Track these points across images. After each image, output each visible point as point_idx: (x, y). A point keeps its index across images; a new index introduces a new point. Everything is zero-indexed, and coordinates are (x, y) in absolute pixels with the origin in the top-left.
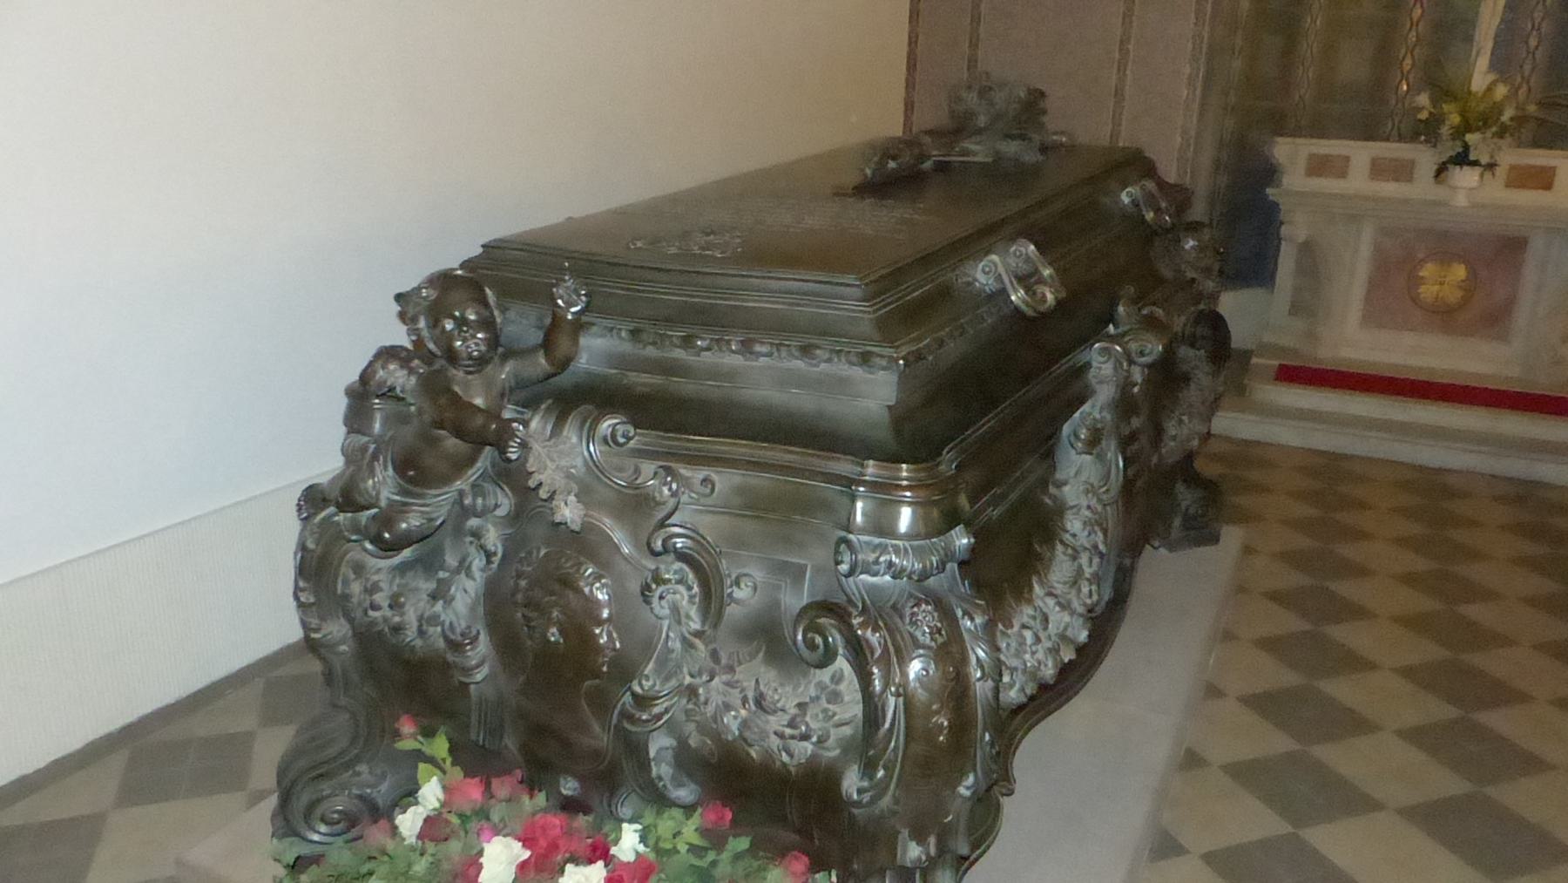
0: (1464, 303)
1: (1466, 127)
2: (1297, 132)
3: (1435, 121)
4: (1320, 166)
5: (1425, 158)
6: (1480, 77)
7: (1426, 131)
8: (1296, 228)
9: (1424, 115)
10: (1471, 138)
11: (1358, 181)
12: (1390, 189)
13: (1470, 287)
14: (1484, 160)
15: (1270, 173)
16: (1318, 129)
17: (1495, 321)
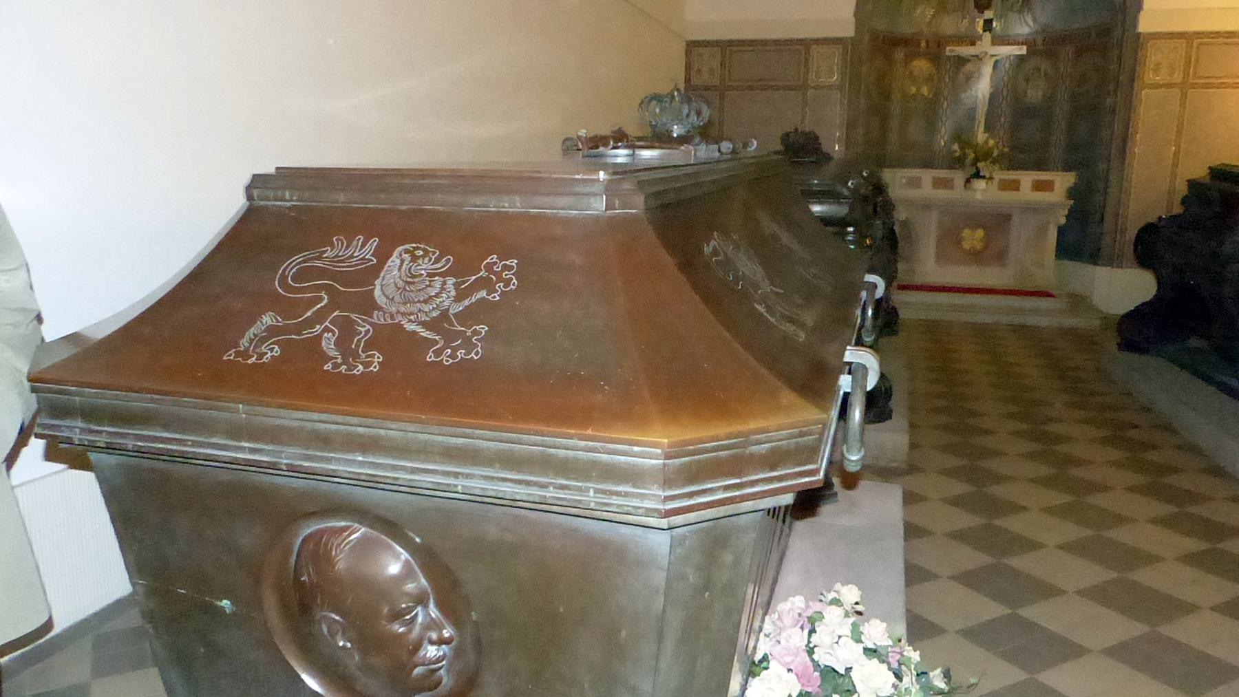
0: (986, 248)
1: (976, 160)
2: (891, 166)
3: (965, 156)
5: (959, 177)
6: (981, 136)
7: (956, 163)
9: (957, 154)
10: (980, 165)
12: (942, 194)
13: (987, 240)
14: (988, 175)
17: (1000, 257)
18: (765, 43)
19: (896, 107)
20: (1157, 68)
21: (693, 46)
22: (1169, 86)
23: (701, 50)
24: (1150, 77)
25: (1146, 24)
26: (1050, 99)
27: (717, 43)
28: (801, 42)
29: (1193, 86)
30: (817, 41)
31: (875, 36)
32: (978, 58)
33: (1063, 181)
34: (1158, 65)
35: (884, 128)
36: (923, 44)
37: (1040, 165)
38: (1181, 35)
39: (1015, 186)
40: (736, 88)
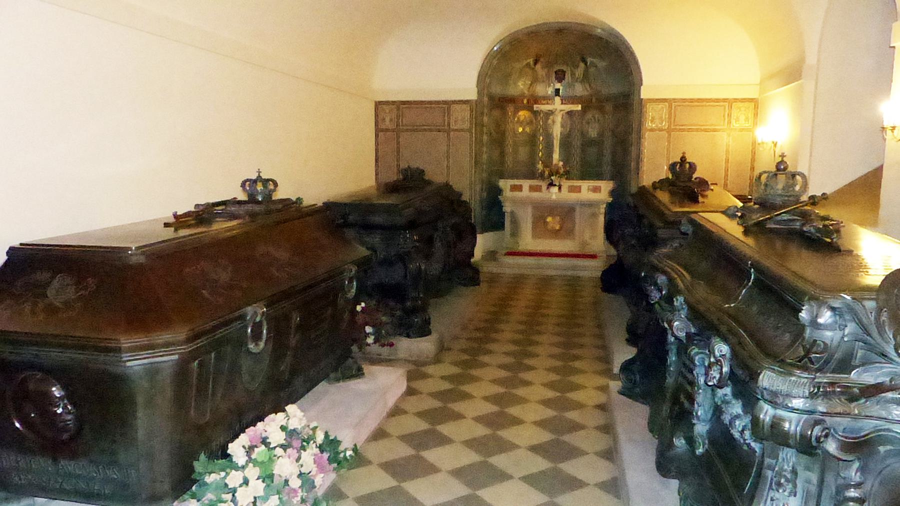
0: (561, 228)
1: (551, 174)
4: (515, 188)
7: (542, 176)
8: (507, 208)
11: (526, 192)
12: (536, 195)
15: (499, 191)
16: (512, 177)
18: (422, 102)
19: (510, 141)
20: (653, 119)
21: (378, 104)
22: (661, 130)
23: (384, 107)
24: (649, 124)
25: (645, 93)
26: (601, 134)
27: (394, 102)
28: (445, 102)
29: (674, 130)
30: (454, 102)
31: (491, 98)
32: (551, 113)
33: (606, 186)
34: (653, 118)
35: (502, 154)
36: (525, 101)
37: (599, 177)
38: (664, 100)
39: (578, 189)
40: (407, 130)
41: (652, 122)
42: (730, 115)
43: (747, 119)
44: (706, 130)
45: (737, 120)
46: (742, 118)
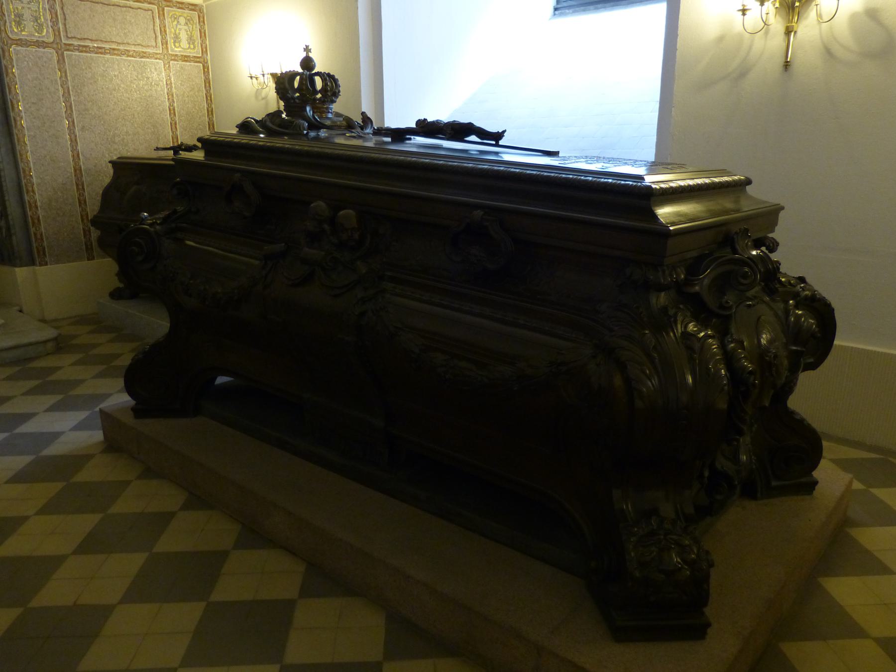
29: (68, 47)
41: (18, 24)
42: (163, 31)
43: (191, 39)
44: (126, 53)
45: (177, 38)
46: (183, 36)
